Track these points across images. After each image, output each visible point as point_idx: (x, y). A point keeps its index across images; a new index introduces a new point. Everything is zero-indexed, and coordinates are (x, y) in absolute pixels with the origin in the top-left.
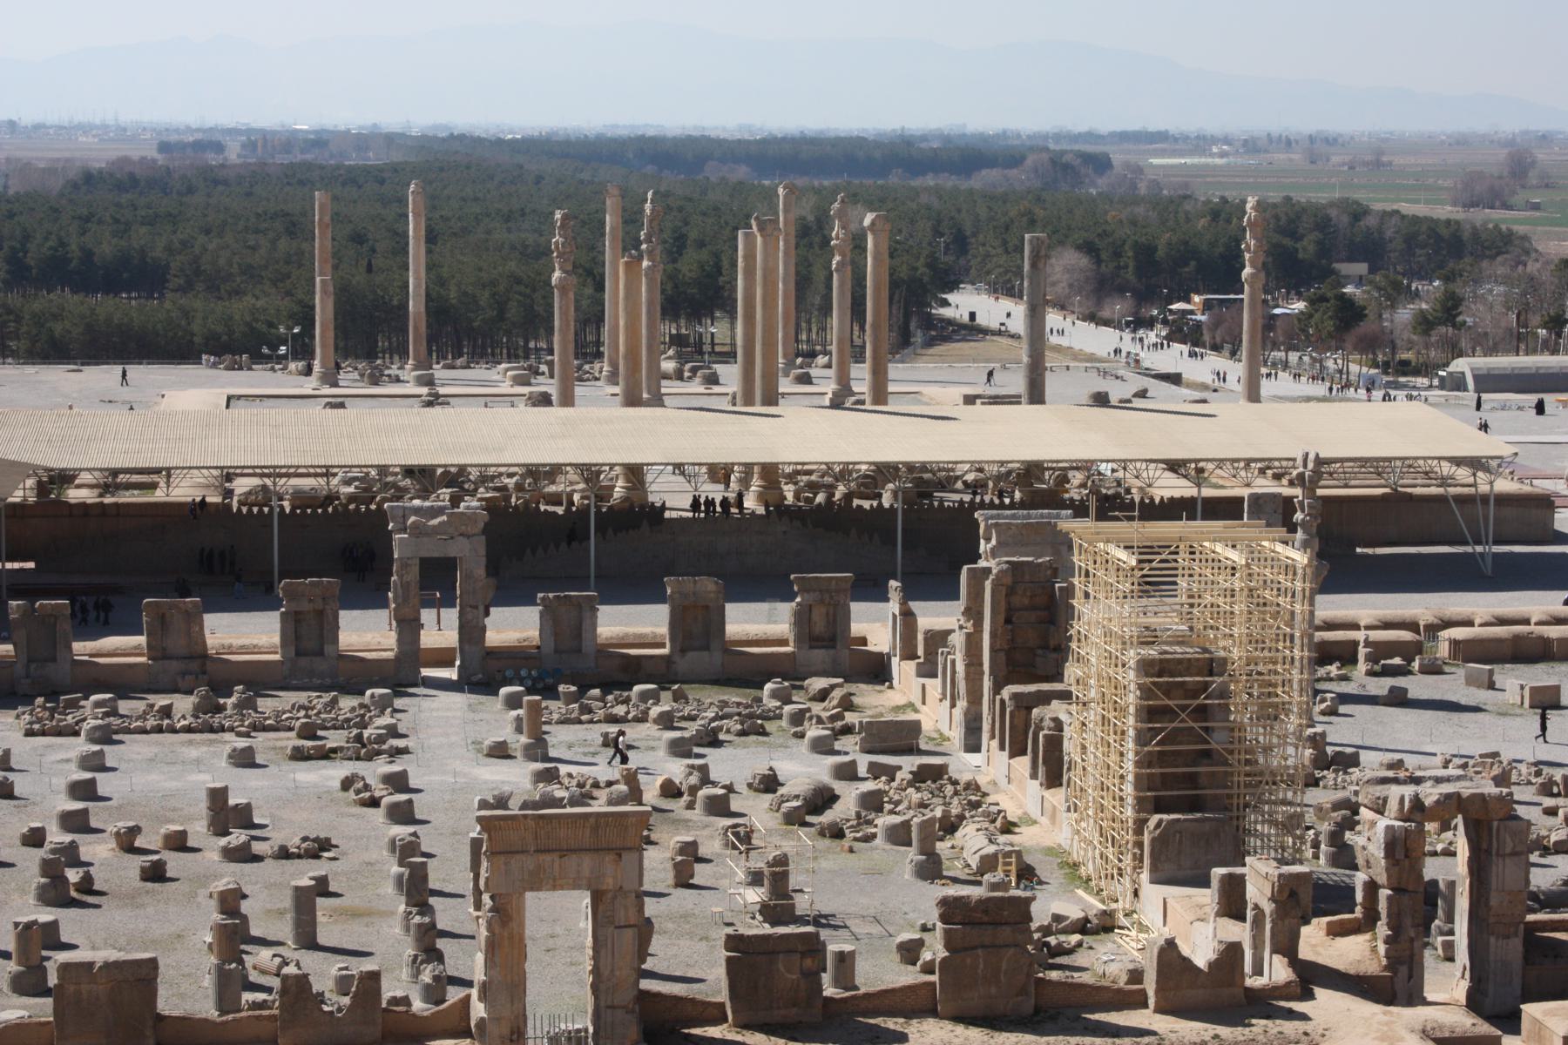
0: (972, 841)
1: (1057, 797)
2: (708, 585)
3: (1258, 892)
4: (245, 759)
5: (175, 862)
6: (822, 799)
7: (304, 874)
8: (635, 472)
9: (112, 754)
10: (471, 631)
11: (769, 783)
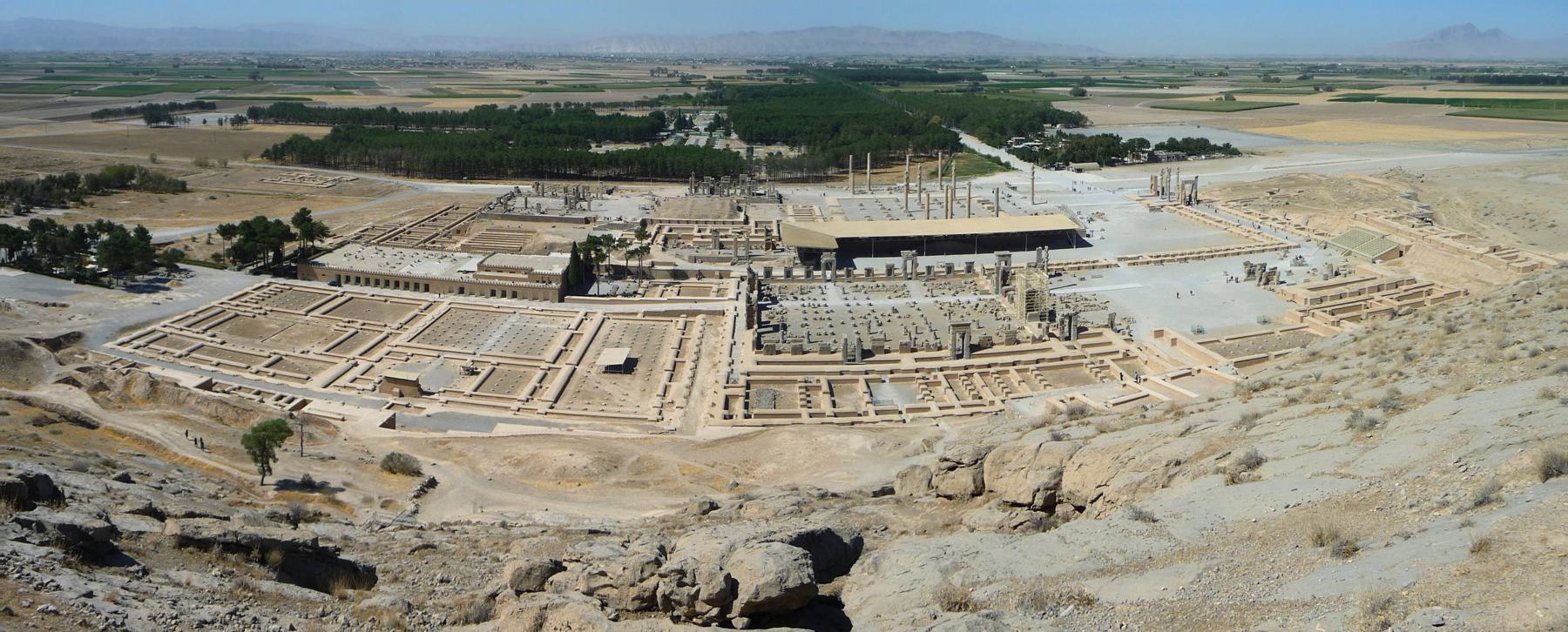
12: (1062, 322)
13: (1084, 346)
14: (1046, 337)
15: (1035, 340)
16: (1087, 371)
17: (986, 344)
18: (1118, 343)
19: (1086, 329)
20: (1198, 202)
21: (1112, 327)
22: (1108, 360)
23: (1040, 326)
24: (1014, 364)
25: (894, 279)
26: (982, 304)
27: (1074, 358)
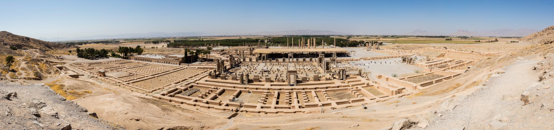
0: (317, 71)
1: (322, 69)
2: (305, 58)
3: (331, 74)
4: (280, 67)
5: (275, 72)
6: (310, 69)
7: (281, 73)
8: (302, 52)
9: (273, 66)
10: (293, 61)
11: (307, 68)
12: (339, 73)
13: (349, 82)
14: (333, 79)
15: (327, 79)
16: (350, 92)
17: (305, 79)
18: (364, 80)
19: (349, 76)
20: (380, 49)
21: (360, 75)
22: (360, 87)
23: (330, 75)
24: (315, 89)
25: (285, 63)
26: (311, 69)
27: (344, 86)
